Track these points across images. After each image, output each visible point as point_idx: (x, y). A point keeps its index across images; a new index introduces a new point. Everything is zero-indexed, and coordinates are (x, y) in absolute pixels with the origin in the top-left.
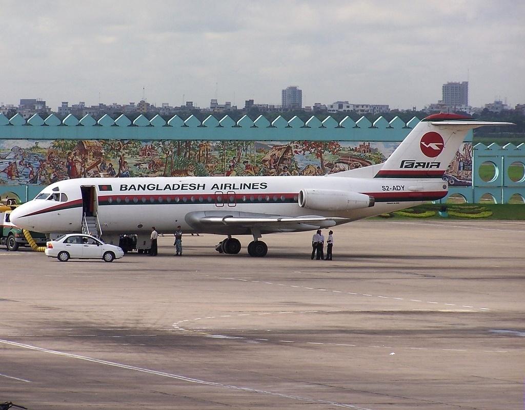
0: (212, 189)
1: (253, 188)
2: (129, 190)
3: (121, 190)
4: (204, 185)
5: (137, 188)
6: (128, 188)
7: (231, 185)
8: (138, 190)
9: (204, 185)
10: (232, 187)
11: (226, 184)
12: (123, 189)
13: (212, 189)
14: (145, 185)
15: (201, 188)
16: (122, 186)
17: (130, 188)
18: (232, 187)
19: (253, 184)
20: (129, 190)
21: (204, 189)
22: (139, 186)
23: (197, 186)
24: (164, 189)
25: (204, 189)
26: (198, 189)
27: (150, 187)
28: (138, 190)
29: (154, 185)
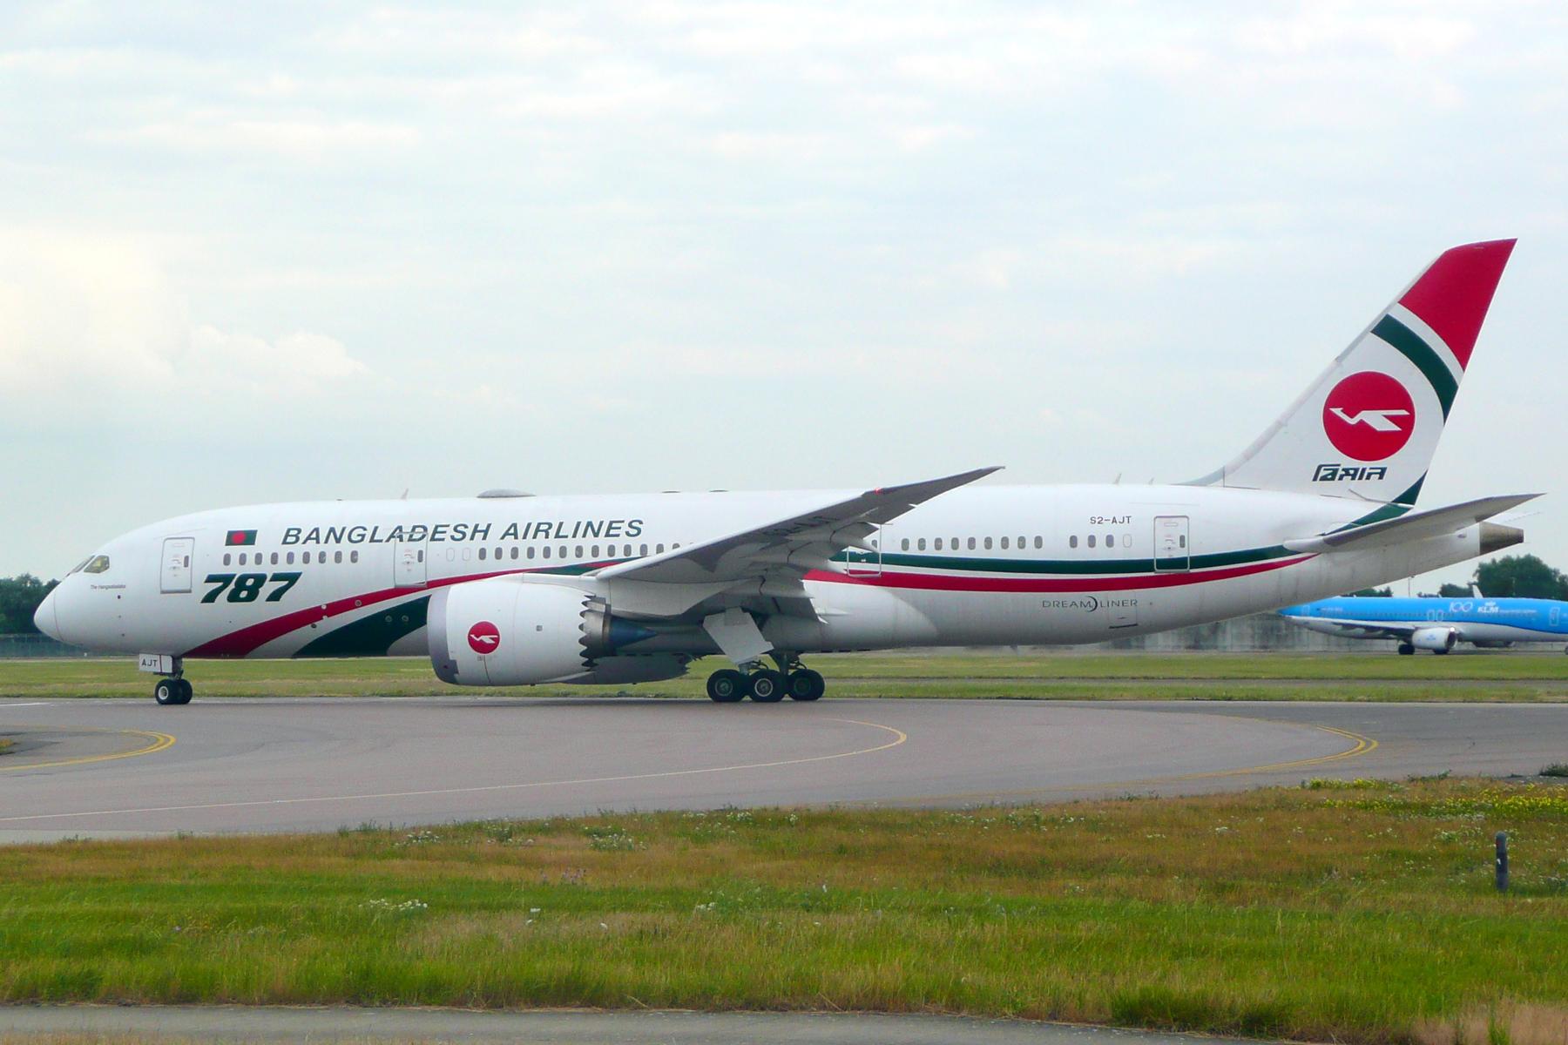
0: (503, 538)
1: (607, 535)
2: (304, 543)
3: (285, 542)
4: (489, 526)
5: (322, 538)
6: (303, 537)
7: (550, 526)
8: (326, 542)
9: (489, 526)
10: (552, 532)
11: (539, 524)
12: (290, 539)
13: (503, 538)
14: (344, 529)
15: (479, 536)
16: (289, 530)
17: (309, 538)
18: (552, 532)
19: (611, 523)
20: (304, 543)
21: (484, 538)
22: (332, 530)
23: (469, 532)
24: (388, 541)
25: (484, 538)
26: (472, 538)
27: (354, 537)
28: (326, 542)
29: (365, 529)
